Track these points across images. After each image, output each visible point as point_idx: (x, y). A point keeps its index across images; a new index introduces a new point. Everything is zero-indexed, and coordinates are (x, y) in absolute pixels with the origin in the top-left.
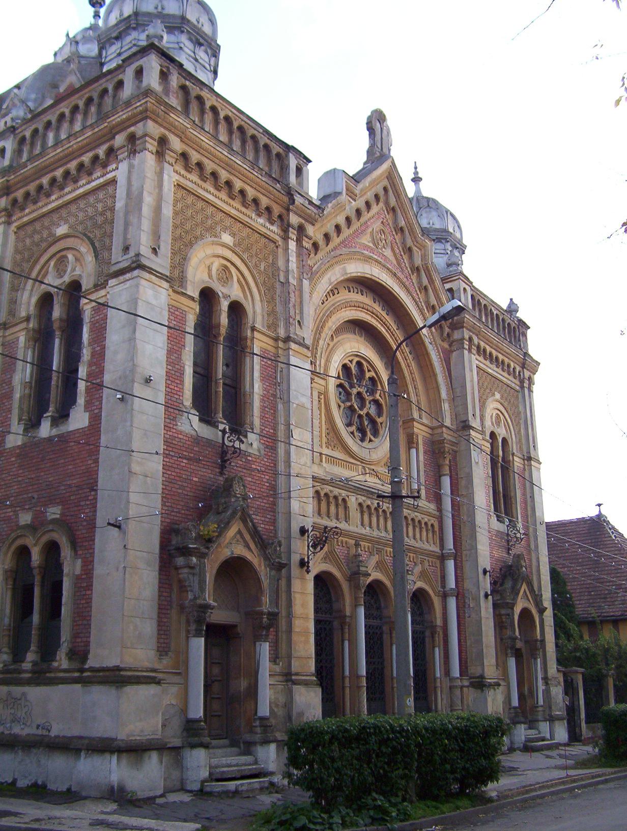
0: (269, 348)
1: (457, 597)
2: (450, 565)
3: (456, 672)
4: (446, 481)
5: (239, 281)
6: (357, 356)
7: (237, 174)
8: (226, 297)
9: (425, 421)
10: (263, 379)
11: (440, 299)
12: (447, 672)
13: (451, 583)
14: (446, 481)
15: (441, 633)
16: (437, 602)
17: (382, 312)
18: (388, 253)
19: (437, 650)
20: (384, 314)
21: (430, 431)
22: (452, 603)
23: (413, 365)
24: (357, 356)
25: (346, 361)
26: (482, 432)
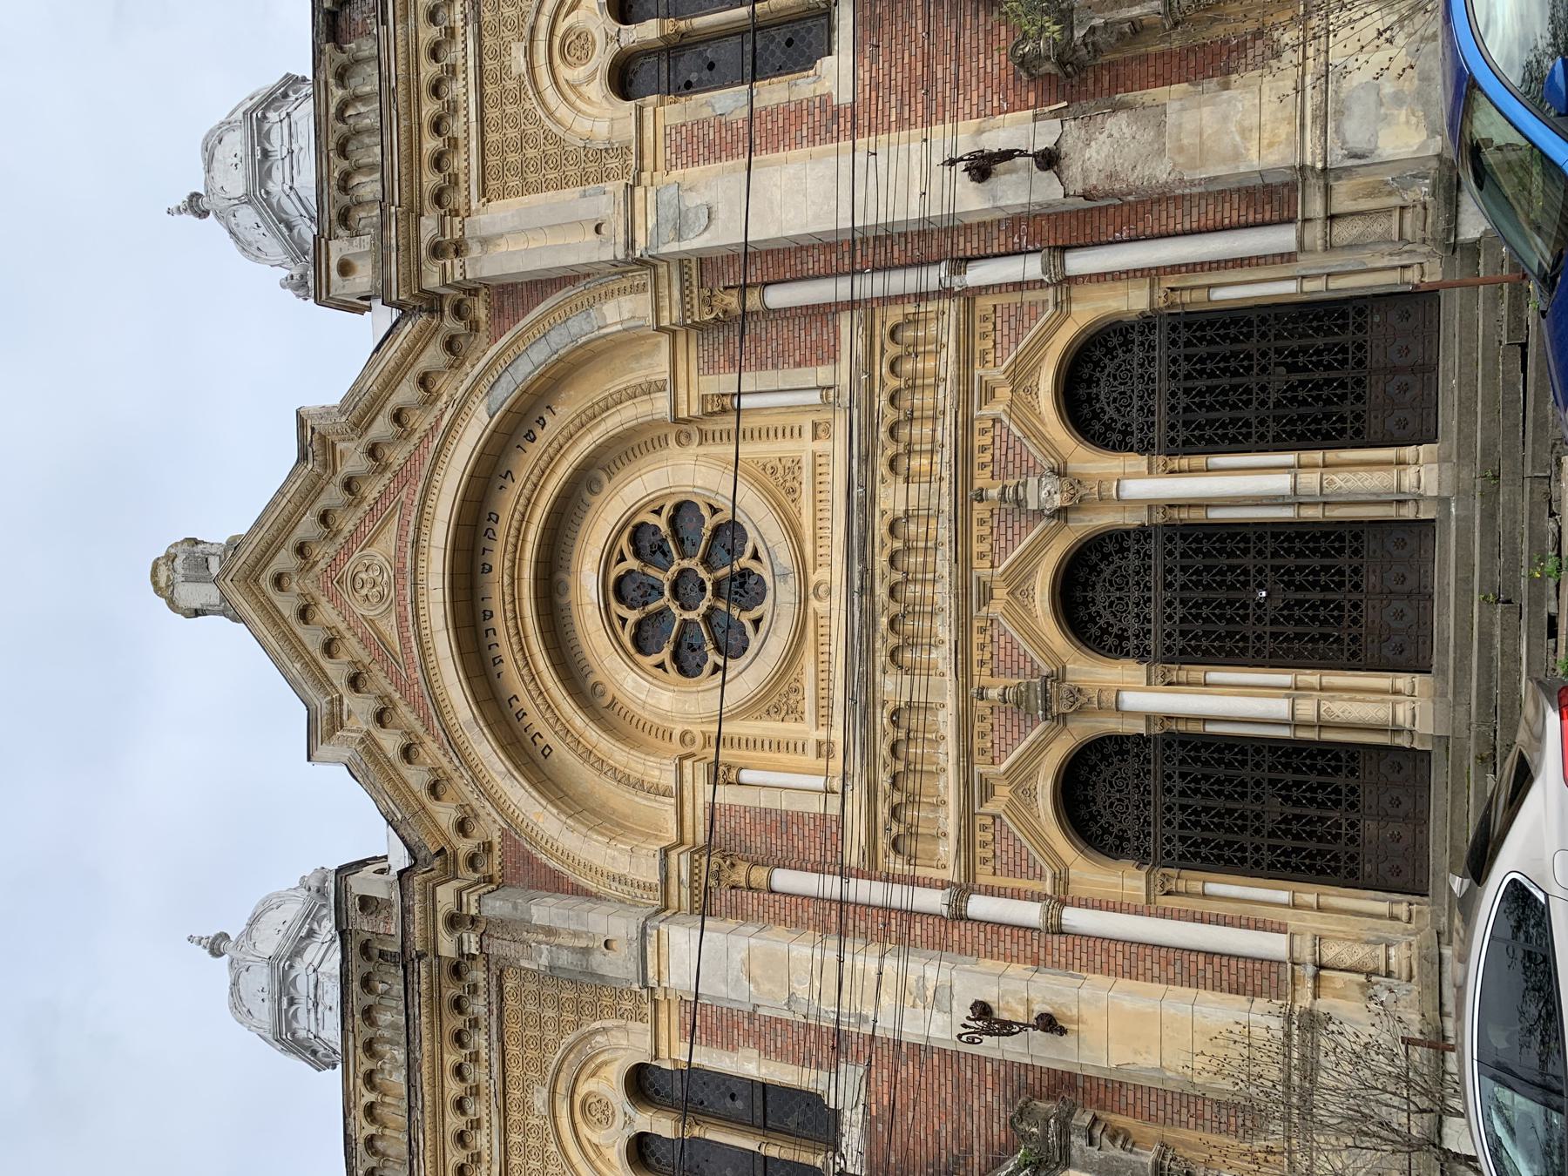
0: (675, 1018)
1: (1064, 249)
2: (978, 274)
3: (1282, 238)
4: (778, 297)
5: (593, 1075)
6: (607, 606)
7: (439, 1136)
8: (629, 1121)
9: (661, 370)
10: (730, 1046)
11: (398, 366)
12: (1286, 257)
13: (1031, 267)
14: (778, 297)
15: (1171, 281)
16: (1088, 310)
17: (501, 537)
18: (384, 548)
19: (1219, 294)
20: (501, 529)
21: (681, 339)
22: (1079, 262)
23: (565, 411)
24: (607, 606)
25: (626, 638)
26: (626, 164)
